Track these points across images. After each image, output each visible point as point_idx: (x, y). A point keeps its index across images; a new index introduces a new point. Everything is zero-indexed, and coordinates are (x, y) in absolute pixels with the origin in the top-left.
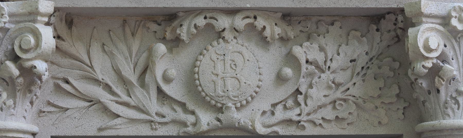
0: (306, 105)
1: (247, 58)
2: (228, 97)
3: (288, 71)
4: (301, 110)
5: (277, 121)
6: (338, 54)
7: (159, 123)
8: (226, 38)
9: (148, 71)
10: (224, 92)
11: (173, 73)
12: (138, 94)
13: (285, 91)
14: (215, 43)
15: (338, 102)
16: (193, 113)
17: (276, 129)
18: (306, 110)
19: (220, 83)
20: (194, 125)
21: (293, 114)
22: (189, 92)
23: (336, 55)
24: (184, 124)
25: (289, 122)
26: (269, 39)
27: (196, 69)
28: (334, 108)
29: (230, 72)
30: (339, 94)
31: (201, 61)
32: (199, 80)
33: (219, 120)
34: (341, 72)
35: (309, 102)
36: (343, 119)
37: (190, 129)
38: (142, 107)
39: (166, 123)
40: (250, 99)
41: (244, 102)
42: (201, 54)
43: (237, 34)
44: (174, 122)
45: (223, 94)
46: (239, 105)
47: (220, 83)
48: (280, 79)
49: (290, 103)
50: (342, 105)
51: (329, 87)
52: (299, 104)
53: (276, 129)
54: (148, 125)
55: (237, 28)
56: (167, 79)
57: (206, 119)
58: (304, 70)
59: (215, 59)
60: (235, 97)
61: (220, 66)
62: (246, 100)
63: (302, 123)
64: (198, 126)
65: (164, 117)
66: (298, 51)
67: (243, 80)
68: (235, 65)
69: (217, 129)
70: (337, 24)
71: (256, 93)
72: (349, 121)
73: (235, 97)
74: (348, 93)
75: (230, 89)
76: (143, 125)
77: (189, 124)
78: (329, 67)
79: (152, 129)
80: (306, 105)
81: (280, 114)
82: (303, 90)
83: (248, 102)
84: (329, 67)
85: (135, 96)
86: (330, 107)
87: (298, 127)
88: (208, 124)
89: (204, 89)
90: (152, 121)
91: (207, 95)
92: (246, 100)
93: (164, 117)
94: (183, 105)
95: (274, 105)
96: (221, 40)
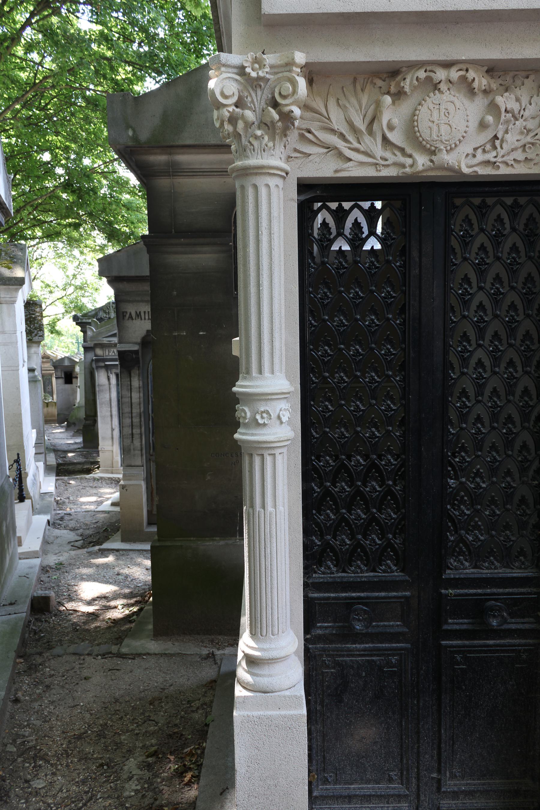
0: (502, 148)
1: (458, 107)
2: (441, 141)
3: (490, 119)
4: (497, 153)
5: (478, 162)
6: (530, 104)
7: (383, 165)
8: (441, 89)
9: (376, 121)
10: (438, 136)
11: (395, 121)
12: (366, 141)
13: (486, 137)
14: (432, 94)
15: (527, 146)
16: (410, 156)
17: (476, 169)
18: (502, 152)
19: (435, 128)
20: (411, 166)
21: (490, 156)
22: (408, 138)
23: (528, 105)
24: (403, 166)
25: (487, 163)
26: (476, 90)
27: (416, 117)
28: (524, 151)
29: (444, 119)
30: (529, 139)
31: (420, 110)
32: (417, 126)
33: (432, 161)
34: (531, 120)
35: (504, 145)
36: (531, 160)
37: (408, 170)
38: (369, 152)
39: (388, 166)
40: (458, 142)
41: (453, 146)
42: (419, 105)
43: (451, 85)
44: (395, 164)
45: (436, 138)
46: (449, 148)
47: (435, 128)
48: (483, 126)
49: (488, 147)
50: (530, 148)
51: (522, 133)
52: (495, 148)
53: (476, 169)
54: (374, 167)
55: (451, 80)
56: (391, 128)
57: (422, 161)
58: (503, 117)
59: (432, 108)
60: (446, 141)
61: (435, 114)
62: (455, 143)
63: (497, 164)
64: (415, 166)
65: (386, 160)
66: (500, 100)
67: (454, 126)
68: (448, 113)
69: (431, 169)
70: (532, 77)
71: (463, 137)
72: (535, 162)
73: (446, 141)
74: (537, 137)
75: (443, 134)
76: (370, 167)
77: (407, 165)
78: (522, 116)
79: (377, 170)
80: (502, 148)
81: (480, 157)
82: (500, 136)
83: (456, 146)
84: (522, 116)
85: (364, 142)
86: (520, 150)
87: (493, 168)
88: (423, 165)
89: (422, 134)
90: (377, 164)
91: (423, 140)
92: (455, 143)
93: (386, 160)
94: (402, 150)
95: (475, 149)
96: (437, 92)
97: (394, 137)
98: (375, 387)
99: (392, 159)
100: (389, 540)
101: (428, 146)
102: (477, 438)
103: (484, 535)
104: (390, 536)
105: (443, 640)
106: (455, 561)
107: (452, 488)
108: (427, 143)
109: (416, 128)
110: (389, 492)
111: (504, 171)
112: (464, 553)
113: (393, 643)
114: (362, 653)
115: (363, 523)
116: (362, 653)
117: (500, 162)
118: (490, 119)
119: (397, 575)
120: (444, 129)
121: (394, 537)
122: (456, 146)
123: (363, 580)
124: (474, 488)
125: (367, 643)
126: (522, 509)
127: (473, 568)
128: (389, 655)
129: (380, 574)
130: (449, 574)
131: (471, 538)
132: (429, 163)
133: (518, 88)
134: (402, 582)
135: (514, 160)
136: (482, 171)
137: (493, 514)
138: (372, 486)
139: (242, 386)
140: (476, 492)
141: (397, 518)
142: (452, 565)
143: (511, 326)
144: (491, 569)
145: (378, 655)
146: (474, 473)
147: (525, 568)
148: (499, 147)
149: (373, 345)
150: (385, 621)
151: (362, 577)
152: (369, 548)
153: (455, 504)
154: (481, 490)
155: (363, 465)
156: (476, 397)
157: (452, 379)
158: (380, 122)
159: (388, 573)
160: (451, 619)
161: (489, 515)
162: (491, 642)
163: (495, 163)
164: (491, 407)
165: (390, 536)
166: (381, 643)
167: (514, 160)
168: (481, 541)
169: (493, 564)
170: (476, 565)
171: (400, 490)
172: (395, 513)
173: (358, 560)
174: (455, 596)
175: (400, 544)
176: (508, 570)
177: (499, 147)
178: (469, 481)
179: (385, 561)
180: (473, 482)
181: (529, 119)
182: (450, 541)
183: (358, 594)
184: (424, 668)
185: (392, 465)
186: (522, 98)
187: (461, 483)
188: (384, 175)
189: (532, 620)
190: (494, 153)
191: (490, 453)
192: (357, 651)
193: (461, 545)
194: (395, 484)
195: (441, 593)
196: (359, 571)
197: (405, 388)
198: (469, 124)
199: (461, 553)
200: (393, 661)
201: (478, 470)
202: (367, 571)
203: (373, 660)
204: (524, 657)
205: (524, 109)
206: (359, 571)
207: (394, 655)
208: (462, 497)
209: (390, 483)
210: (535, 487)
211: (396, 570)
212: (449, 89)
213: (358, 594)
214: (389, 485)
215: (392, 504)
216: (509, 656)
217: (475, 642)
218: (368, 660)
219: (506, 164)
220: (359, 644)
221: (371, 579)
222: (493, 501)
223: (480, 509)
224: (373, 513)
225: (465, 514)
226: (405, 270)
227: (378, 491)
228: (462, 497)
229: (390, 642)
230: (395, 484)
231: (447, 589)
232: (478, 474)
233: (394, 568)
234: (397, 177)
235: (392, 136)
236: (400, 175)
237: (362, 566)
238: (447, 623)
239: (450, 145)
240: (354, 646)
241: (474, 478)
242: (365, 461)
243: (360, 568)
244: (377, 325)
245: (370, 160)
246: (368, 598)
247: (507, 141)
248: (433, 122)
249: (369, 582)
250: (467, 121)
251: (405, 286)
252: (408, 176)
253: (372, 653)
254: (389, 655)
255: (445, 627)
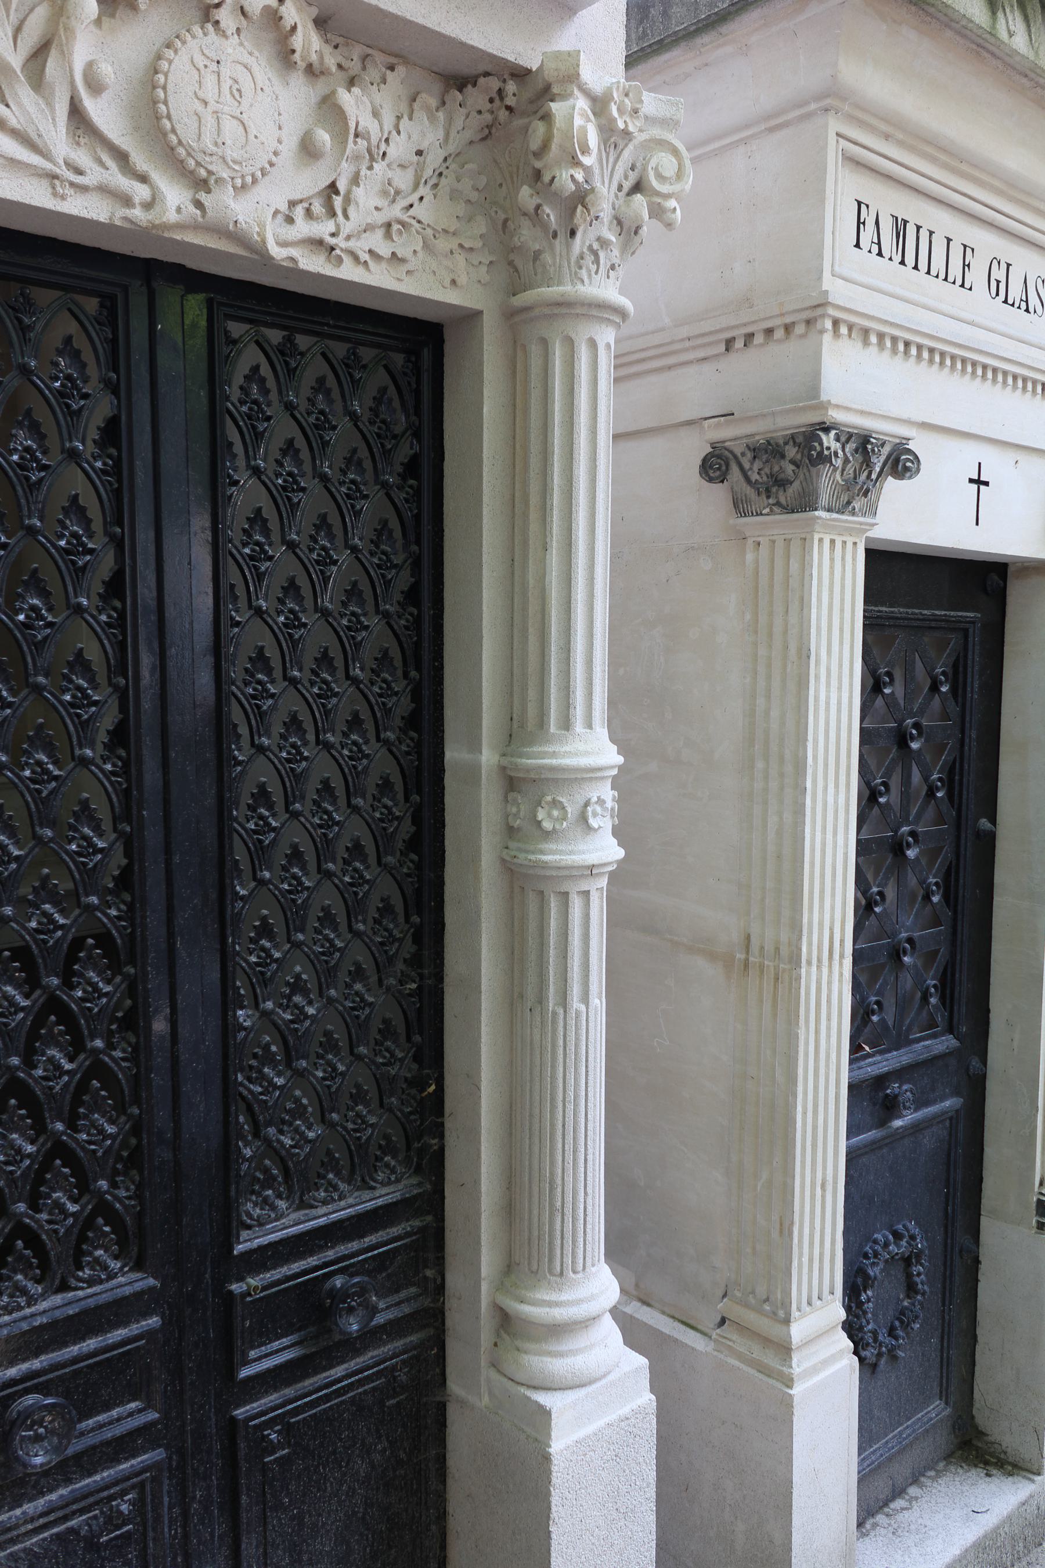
0: (346, 216)
1: (259, 85)
2: (223, 158)
3: (324, 137)
4: (338, 226)
5: (300, 236)
6: (399, 133)
7: (72, 184)
8: (223, 25)
10: (216, 144)
11: (106, 70)
12: (26, 101)
13: (309, 182)
14: (197, 29)
15: (396, 227)
16: (143, 179)
17: (294, 252)
18: (347, 228)
19: (209, 122)
20: (148, 206)
21: (323, 229)
22: (136, 129)
23: (394, 133)
24: (127, 201)
25: (317, 243)
26: (297, 57)
27: (161, 78)
28: (388, 235)
29: (229, 106)
30: (396, 211)
31: (170, 62)
32: (165, 103)
33: (199, 204)
34: (398, 170)
35: (352, 211)
36: (403, 261)
37: (137, 213)
38: (34, 136)
39: (83, 189)
40: (259, 174)
41: (249, 179)
42: (168, 46)
43: (244, 22)
44: (103, 189)
45: (212, 148)
46: (239, 182)
47: (209, 122)
48: (308, 150)
49: (318, 208)
50: (400, 232)
51: (384, 193)
52: (332, 214)
53: (294, 252)
54: (45, 183)
55: (247, 8)
57: (175, 199)
58: (350, 144)
60: (235, 162)
61: (210, 80)
62: (253, 175)
63: (338, 252)
64: (157, 208)
65: (80, 172)
66: (346, 98)
67: (253, 131)
68: (239, 90)
69: (196, 227)
70: (401, 70)
71: (272, 165)
72: (409, 266)
73: (235, 162)
74: (412, 212)
75: (228, 142)
76: (35, 181)
77: (137, 200)
78: (384, 154)
79: (55, 194)
80: (346, 216)
81: (303, 228)
82: (342, 186)
83: (255, 181)
84: (384, 154)
85: (20, 105)
86: (380, 233)
87: (328, 259)
88: (179, 210)
89: (177, 127)
90: (55, 177)
91: (180, 143)
92: (253, 175)
93: (80, 172)
94: (122, 157)
95: (292, 204)
96: (209, 26)
97: (102, 112)
98: (51, 793)
99: (94, 176)
100: (100, 1194)
101: (191, 163)
102: (294, 901)
103: (315, 1127)
104: (103, 1184)
105: (238, 1406)
106: (256, 1204)
107: (245, 1029)
108: (189, 154)
109: (163, 107)
110: (97, 1069)
111: (348, 272)
112: (274, 1178)
113: (119, 1462)
114: (42, 1521)
115: (29, 1167)
116: (42, 1521)
117: (342, 250)
118: (324, 137)
119: (129, 1282)
120: (230, 127)
121: (114, 1185)
122: (255, 181)
123: (37, 1324)
124: (292, 1022)
125: (51, 1491)
126: (387, 1050)
127: (295, 1211)
128: (111, 1498)
129: (80, 1293)
130: (246, 1243)
131: (288, 1142)
132: (192, 209)
133: (375, 86)
134: (138, 1295)
135: (370, 251)
136: (312, 263)
137: (333, 1073)
138: (51, 1060)
139: (815, 1370)
140: (296, 1030)
141: (118, 1134)
142: (252, 1218)
143: (353, 637)
144: (333, 1200)
145: (82, 1511)
146: (288, 984)
147: (398, 1181)
148: (339, 212)
149: (41, 679)
150: (98, 1413)
151: (33, 1315)
152: (47, 1232)
153: (251, 1067)
154: (307, 1023)
155: (23, 1009)
156: (287, 804)
157: (240, 763)
158: (66, 56)
159: (101, 1282)
160: (253, 1348)
161: (324, 1079)
162: (339, 1371)
163: (333, 249)
164: (321, 826)
165: (103, 1184)
166: (90, 1475)
167: (370, 251)
168: (310, 1141)
169: (335, 1188)
170: (302, 1200)
171: (123, 1059)
172: (112, 1121)
173: (15, 1272)
174: (264, 1288)
175: (129, 1198)
176: (367, 1195)
177: (339, 212)
178: (280, 1006)
179: (90, 1254)
180: (288, 1006)
181: (395, 166)
182: (245, 1160)
183: (25, 1367)
184: (198, 1494)
185: (102, 995)
186: (383, 112)
187: (265, 1014)
188: (74, 212)
189: (413, 1290)
190: (330, 226)
191: (320, 933)
192: (26, 1522)
193: (267, 1162)
194: (110, 1046)
195: (231, 1292)
196: (22, 1301)
197: (127, 792)
198: (284, 134)
199: (269, 1181)
200: (124, 1508)
201: (298, 977)
202: (43, 1296)
203: (72, 1530)
204: (404, 1378)
205: (387, 140)
206: (22, 1301)
207: (124, 1493)
208: (267, 1047)
209: (99, 1043)
210: (410, 995)
211: (121, 1269)
212: (238, 30)
213: (25, 1367)
214: (95, 1051)
215: (104, 1098)
216: (374, 1389)
217: (307, 1382)
218: (57, 1535)
219: (356, 258)
220: (31, 1500)
221: (58, 1314)
222: (330, 1045)
223: (305, 1069)
224: (54, 1133)
225: (276, 1087)
226: (120, 481)
227: (68, 1072)
228: (267, 1047)
229: (116, 1460)
230: (110, 1046)
231: (241, 1279)
232: (298, 986)
233: (115, 1265)
234: (108, 228)
235: (95, 109)
236: (118, 223)
237: (30, 1285)
238: (246, 1363)
239: (243, 177)
240: (18, 1512)
241: (289, 998)
242: (27, 996)
243: (24, 1292)
244: (50, 625)
245: (35, 159)
246: (54, 1367)
247: (357, 203)
248: (206, 103)
249: (53, 1325)
250: (280, 128)
251: (121, 525)
252: (136, 232)
253: (67, 1511)
254: (111, 1498)
255: (245, 1372)
